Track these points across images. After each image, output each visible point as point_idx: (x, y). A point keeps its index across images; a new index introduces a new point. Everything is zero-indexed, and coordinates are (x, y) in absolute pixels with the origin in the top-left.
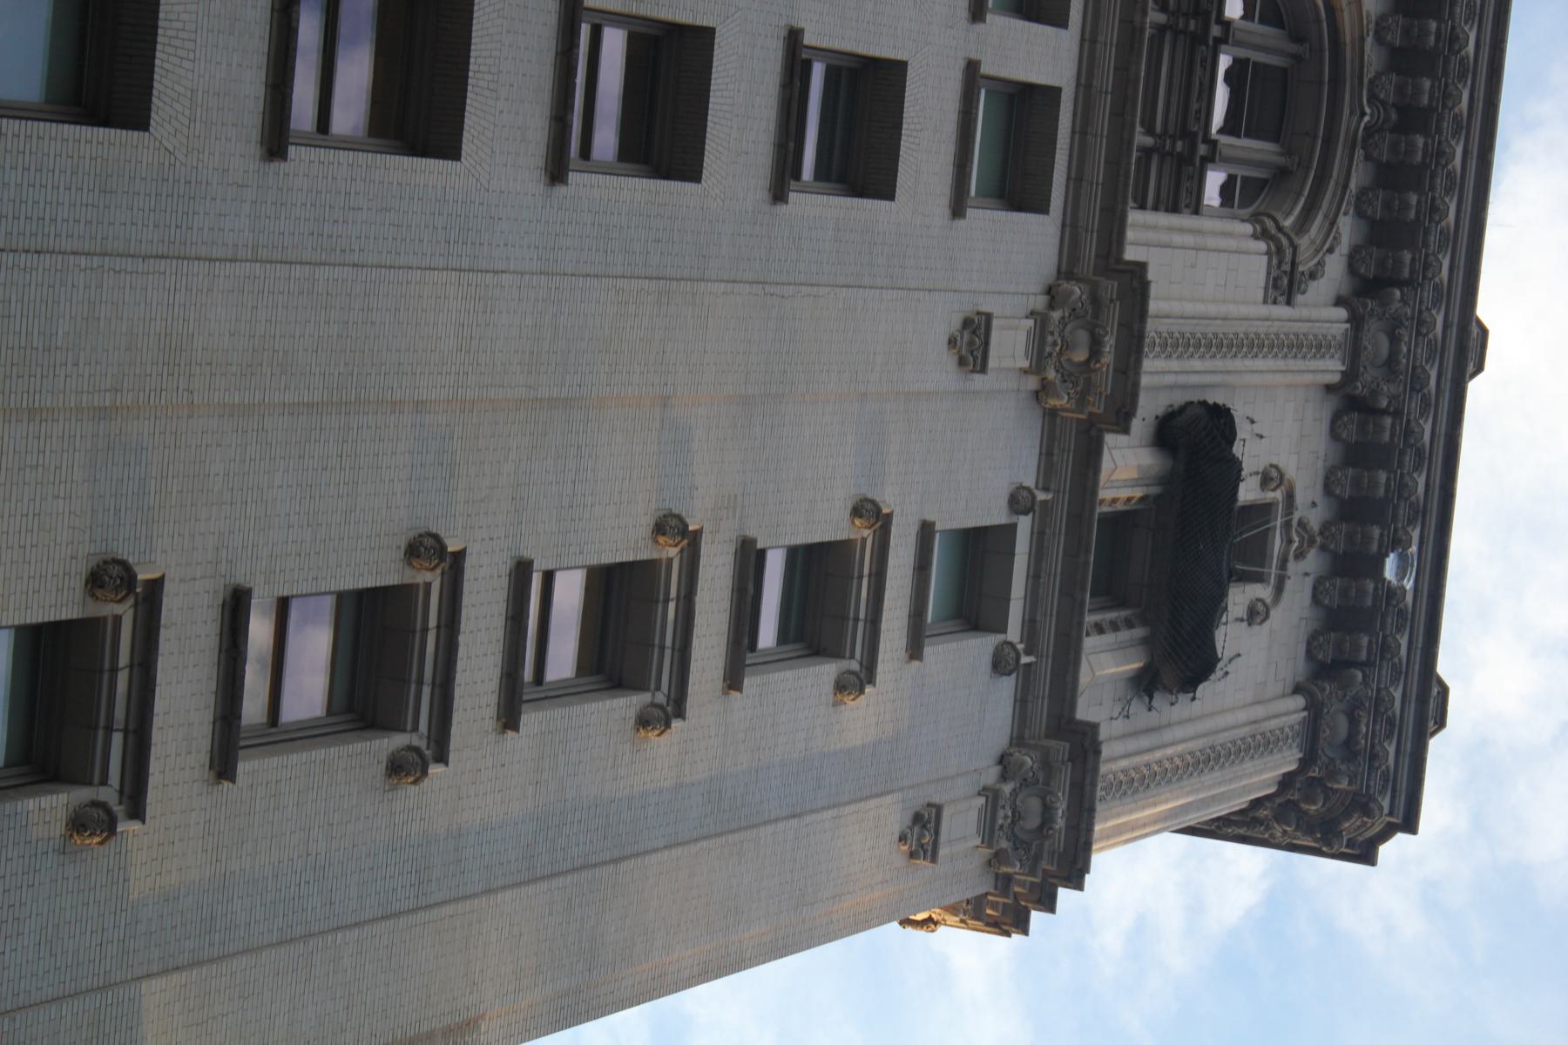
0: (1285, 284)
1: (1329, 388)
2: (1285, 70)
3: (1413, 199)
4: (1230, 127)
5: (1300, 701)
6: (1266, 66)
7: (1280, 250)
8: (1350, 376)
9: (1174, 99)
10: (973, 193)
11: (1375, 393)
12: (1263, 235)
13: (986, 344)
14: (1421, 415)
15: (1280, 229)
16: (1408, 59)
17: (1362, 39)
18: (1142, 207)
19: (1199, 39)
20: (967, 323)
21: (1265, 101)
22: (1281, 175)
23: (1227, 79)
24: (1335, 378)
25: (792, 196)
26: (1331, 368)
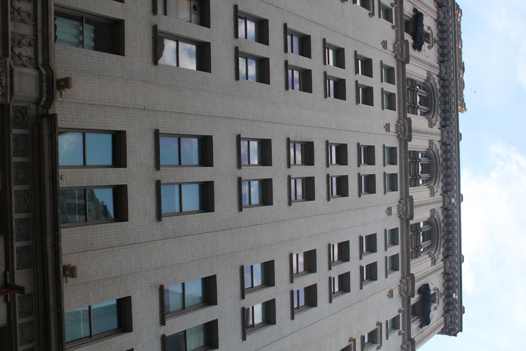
0: (432, 194)
1: (441, 207)
4: (422, 173)
11: (448, 207)
12: (429, 187)
19: (416, 162)
21: (427, 169)
26: (441, 205)
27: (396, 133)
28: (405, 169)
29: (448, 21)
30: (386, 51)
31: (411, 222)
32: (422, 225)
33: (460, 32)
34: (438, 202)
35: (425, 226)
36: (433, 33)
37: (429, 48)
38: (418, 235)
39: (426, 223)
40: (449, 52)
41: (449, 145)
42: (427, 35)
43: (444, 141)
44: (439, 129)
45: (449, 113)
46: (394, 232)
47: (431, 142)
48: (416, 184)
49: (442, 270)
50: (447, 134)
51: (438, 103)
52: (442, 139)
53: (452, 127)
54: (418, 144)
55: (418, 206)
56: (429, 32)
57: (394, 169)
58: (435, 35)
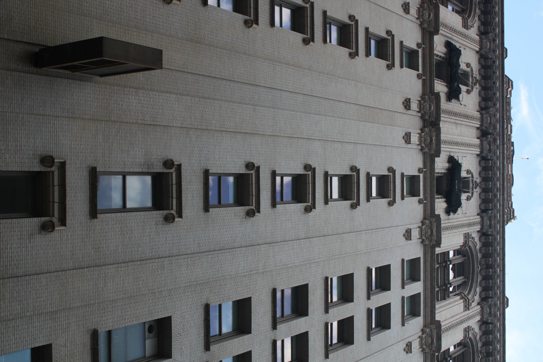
0: (467, 307)
2: (463, 262)
5: (479, 307)
7: (466, 300)
8: (482, 228)
11: (488, 320)
15: (465, 296)
16: (486, 256)
18: (438, 301)
19: (445, 262)
20: (406, 231)
21: (459, 270)
22: (464, 282)
24: (479, 229)
25: (371, 200)
26: (478, 228)
27: (418, 145)
28: (431, 275)
29: (495, 153)
30: (409, 146)
31: (438, 250)
32: (452, 349)
34: (473, 224)
35: (456, 257)
36: (474, 72)
37: (468, 92)
39: (457, 252)
40: (495, 196)
41: (492, 235)
42: (466, 74)
43: (484, 155)
44: (478, 138)
45: (492, 246)
46: (414, 263)
47: (467, 236)
48: (445, 295)
49: (478, 318)
50: (488, 222)
51: (478, 268)
52: (482, 152)
53: (496, 211)
54: (451, 242)
55: (447, 228)
56: (469, 69)
57: (417, 288)
58: (476, 73)
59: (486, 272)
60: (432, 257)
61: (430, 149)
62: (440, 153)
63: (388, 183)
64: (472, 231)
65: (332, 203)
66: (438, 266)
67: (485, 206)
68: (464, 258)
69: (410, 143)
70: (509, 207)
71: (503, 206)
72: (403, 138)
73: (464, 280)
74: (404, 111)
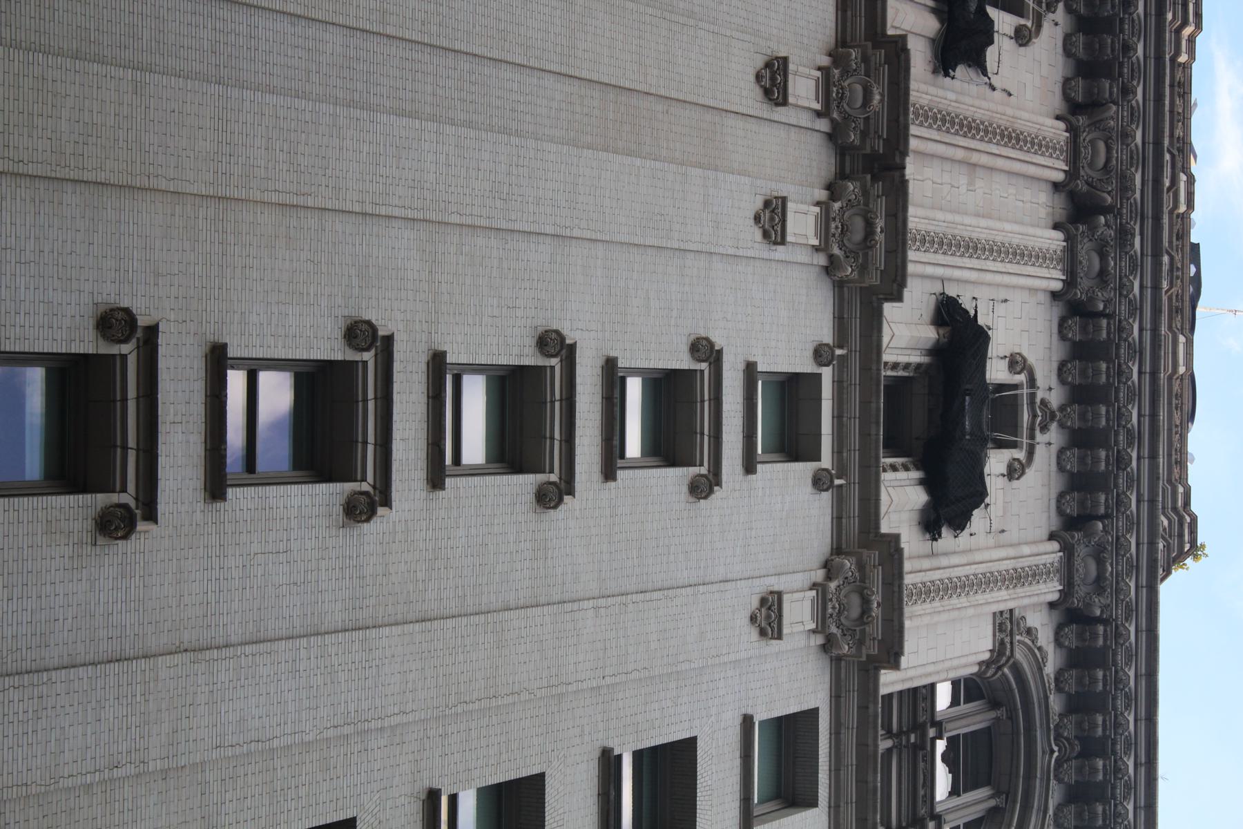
2: (988, 730)
3: (1100, 763)
6: (972, 732)
8: (1066, 593)
9: (904, 773)
10: (759, 451)
13: (780, 616)
14: (1127, 620)
16: (1082, 704)
17: (1046, 698)
19: (919, 728)
20: (763, 601)
22: (993, 812)
23: (943, 760)
25: (620, 474)
27: (817, 249)
30: (780, 252)
31: (890, 681)
33: (1182, 400)
35: (963, 708)
37: (1022, 37)
38: (923, 752)
39: (966, 689)
40: (1121, 461)
41: (1105, 622)
45: (1105, 667)
46: (791, 732)
47: (1006, 624)
51: (1047, 754)
55: (928, 592)
59: (1080, 770)
60: (863, 708)
61: (863, 269)
62: (902, 284)
63: (691, 402)
64: (1026, 601)
65: (461, 481)
66: (888, 744)
67: (1082, 503)
68: (992, 714)
69: (783, 242)
70: (1175, 509)
71: (1152, 501)
72: (757, 219)
73: (992, 803)
74: (764, 110)
